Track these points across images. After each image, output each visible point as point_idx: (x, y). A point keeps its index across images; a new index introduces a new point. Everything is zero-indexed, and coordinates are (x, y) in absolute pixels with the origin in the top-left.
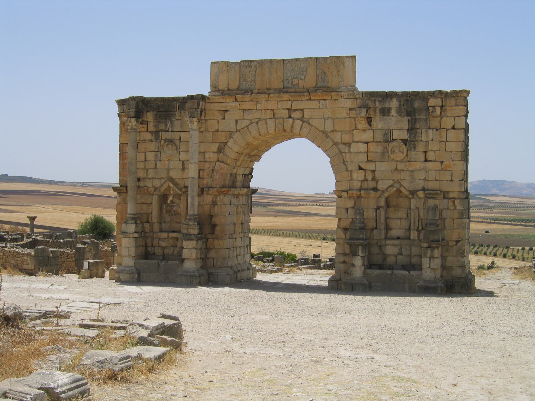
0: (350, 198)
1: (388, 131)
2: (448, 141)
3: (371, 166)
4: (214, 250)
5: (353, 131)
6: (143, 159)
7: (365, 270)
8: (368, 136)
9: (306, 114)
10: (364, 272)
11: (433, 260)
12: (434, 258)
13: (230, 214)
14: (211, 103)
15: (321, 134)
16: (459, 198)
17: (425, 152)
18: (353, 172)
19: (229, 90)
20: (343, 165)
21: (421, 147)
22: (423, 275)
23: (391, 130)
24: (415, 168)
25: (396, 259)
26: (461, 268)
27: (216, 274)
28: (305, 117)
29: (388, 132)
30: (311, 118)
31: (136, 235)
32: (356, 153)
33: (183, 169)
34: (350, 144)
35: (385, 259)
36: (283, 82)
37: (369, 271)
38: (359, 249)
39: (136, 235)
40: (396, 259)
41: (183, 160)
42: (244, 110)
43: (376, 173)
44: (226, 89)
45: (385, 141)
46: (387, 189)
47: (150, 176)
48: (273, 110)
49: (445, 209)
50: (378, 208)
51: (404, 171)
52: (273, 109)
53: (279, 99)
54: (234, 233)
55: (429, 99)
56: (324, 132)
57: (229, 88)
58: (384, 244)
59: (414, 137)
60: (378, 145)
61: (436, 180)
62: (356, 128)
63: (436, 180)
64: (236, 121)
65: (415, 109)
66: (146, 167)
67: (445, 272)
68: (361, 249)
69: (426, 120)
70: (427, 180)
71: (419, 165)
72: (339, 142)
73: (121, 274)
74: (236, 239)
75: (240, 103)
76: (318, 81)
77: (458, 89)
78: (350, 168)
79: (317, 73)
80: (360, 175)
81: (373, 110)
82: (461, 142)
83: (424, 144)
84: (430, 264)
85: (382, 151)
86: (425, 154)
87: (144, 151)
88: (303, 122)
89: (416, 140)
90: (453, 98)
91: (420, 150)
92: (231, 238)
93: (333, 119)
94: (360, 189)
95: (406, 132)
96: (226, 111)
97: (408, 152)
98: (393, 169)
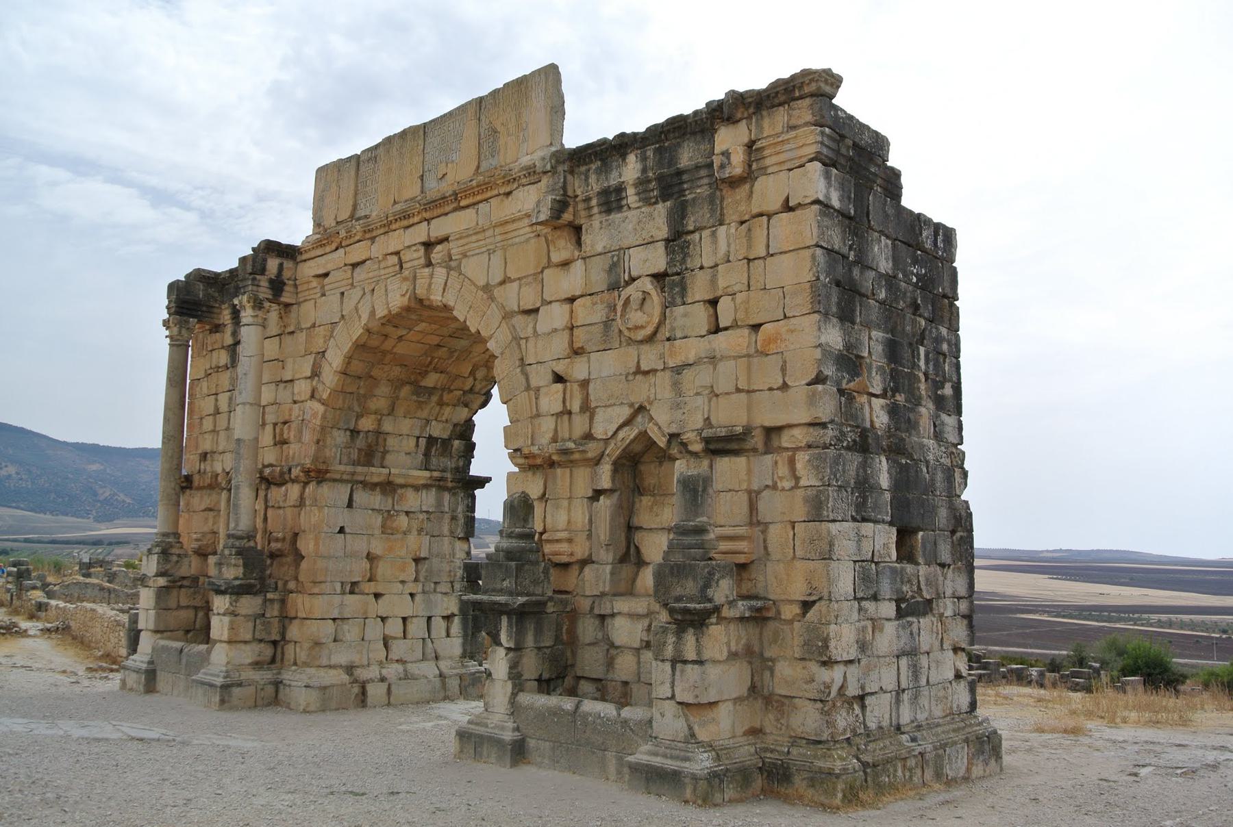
1: (618, 256)
2: (772, 255)
3: (579, 370)
4: (296, 622)
5: (542, 272)
6: (211, 411)
7: (514, 695)
8: (574, 280)
11: (682, 671)
12: (685, 662)
13: (347, 530)
14: (305, 261)
15: (480, 293)
16: (809, 446)
17: (714, 303)
18: (543, 391)
19: (337, 223)
20: (520, 374)
21: (699, 289)
22: (654, 723)
23: (626, 251)
24: (683, 359)
25: (639, 663)
26: (819, 705)
27: (288, 682)
28: (453, 258)
29: (619, 260)
30: (465, 256)
31: (162, 581)
32: (549, 334)
35: (610, 664)
36: (422, 180)
37: (525, 698)
38: (502, 623)
39: (162, 581)
40: (639, 663)
42: (355, 266)
43: (591, 386)
44: (334, 224)
45: (614, 287)
46: (616, 433)
47: (221, 448)
48: (397, 253)
49: (767, 486)
50: (598, 494)
51: (659, 374)
52: (397, 249)
53: (405, 223)
54: (370, 580)
55: (716, 131)
56: (487, 288)
57: (339, 220)
58: (608, 611)
59: (683, 261)
60: (596, 303)
61: (738, 390)
62: (549, 264)
63: (738, 390)
64: (342, 294)
65: (680, 173)
66: (217, 429)
67: (771, 716)
68: (506, 624)
69: (711, 199)
70: (717, 396)
71: (691, 349)
72: (516, 312)
74: (377, 596)
75: (347, 249)
76: (482, 158)
77: (786, 74)
78: (534, 383)
79: (479, 135)
80: (551, 399)
81: (584, 201)
82: (808, 247)
83: (708, 277)
84: (673, 687)
85: (604, 319)
86: (711, 310)
87: (214, 392)
88: (449, 269)
89: (686, 269)
90: (781, 108)
91: (697, 300)
92: (352, 592)
94: (555, 440)
95: (661, 246)
96: (326, 275)
97: (668, 310)
98: (631, 371)
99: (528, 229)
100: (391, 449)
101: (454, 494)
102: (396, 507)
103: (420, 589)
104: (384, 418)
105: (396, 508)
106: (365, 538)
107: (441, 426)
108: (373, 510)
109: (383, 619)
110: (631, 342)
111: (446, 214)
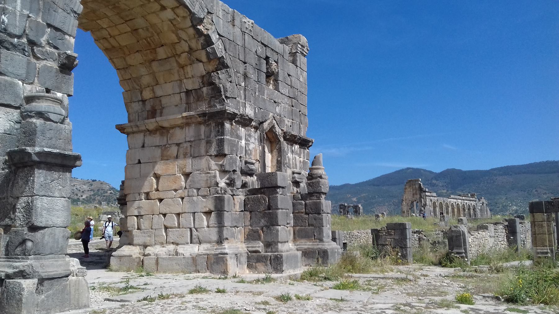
100: (165, 105)
101: (208, 125)
102: (169, 143)
103: (186, 194)
104: (154, 87)
105: (169, 143)
106: (151, 164)
107: (190, 81)
108: (156, 146)
109: (165, 215)
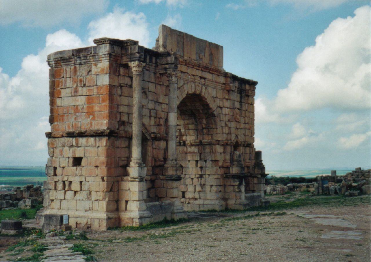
0: (223, 145)
3: (229, 125)
5: (223, 99)
8: (228, 104)
9: (207, 84)
10: (245, 197)
18: (224, 127)
30: (208, 85)
33: (150, 117)
34: (221, 108)
41: (151, 108)
43: (231, 129)
48: (193, 75)
56: (213, 97)
61: (248, 135)
63: (248, 135)
73: (143, 219)
93: (217, 89)
99: (220, 87)
110: (236, 121)
111: (206, 72)
